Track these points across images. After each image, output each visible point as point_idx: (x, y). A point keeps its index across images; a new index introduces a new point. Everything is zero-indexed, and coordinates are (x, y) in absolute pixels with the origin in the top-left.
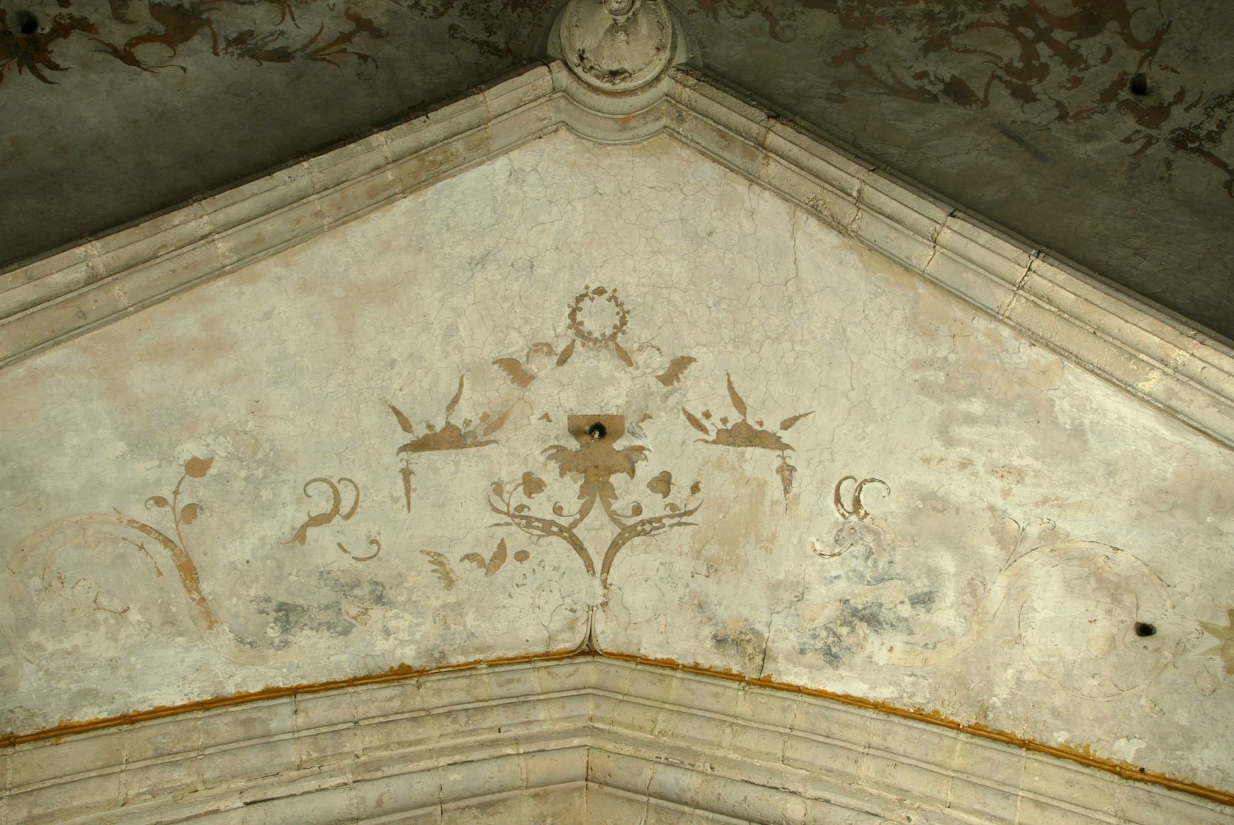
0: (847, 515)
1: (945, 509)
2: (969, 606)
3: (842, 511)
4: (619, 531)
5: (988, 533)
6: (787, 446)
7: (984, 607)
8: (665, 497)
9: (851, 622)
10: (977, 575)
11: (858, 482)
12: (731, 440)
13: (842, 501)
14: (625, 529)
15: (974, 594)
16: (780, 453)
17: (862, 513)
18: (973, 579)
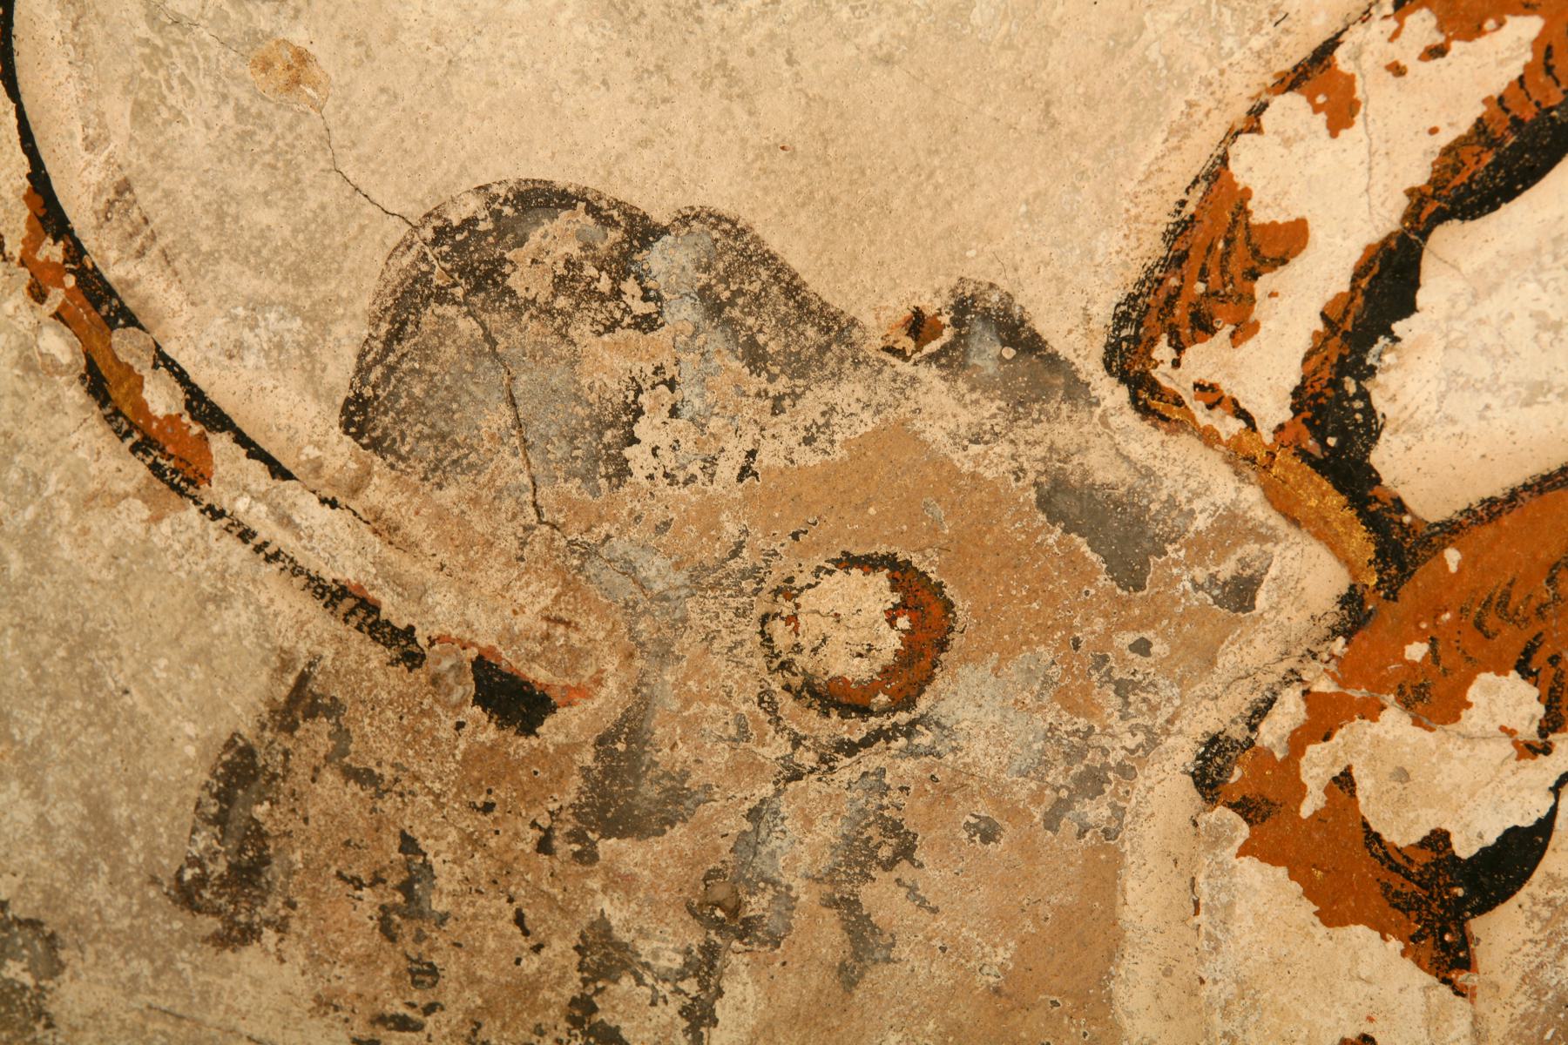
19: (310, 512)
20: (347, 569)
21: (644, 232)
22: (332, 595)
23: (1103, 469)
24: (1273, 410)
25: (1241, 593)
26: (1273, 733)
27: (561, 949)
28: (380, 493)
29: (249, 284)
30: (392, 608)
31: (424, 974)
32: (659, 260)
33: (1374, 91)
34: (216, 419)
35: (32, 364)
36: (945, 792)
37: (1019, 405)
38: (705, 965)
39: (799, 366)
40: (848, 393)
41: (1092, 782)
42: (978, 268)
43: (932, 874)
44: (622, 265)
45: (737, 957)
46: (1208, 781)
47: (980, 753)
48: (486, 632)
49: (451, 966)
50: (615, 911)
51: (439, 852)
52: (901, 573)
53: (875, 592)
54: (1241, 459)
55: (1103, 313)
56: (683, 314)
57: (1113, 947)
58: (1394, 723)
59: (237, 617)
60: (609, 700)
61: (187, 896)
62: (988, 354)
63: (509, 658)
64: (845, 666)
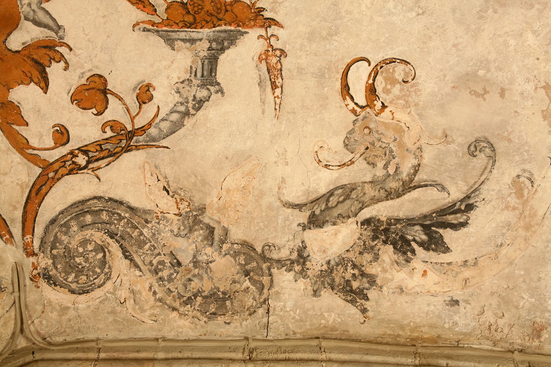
0: (359, 110)
1: (486, 92)
2: (514, 209)
3: (352, 105)
4: (38, 171)
5: (539, 118)
6: (272, 22)
7: (532, 208)
8: (99, 114)
9: (372, 248)
10: (524, 171)
11: (373, 64)
12: (189, 19)
13: (351, 92)
14: (47, 166)
15: (519, 193)
16: (262, 32)
17: (378, 105)
18: (518, 176)
19: (356, 156)
20: (359, 155)
21: (347, 137)
22: (360, 156)
23: (362, 118)
24: (361, 110)
25: (368, 113)
26: (375, 113)
27: (380, 149)
28: (356, 153)
29: (345, 157)
30: (362, 153)
31: (380, 156)
32: (348, 136)
33: (348, 103)
34: (351, 160)
35: (346, 169)
36: (375, 128)
37: (358, 121)
38: (382, 142)
39: (354, 131)
40: (356, 129)
41: (376, 121)
42: (352, 122)
43: (379, 130)
44: (348, 138)
45: (382, 140)
46: (377, 116)
47: (374, 126)
48: (364, 149)
49: (380, 155)
50: (378, 146)
51: (374, 154)
52: (365, 128)
53: (365, 130)
54: (362, 112)
55: (354, 116)
56: (351, 136)
57: (384, 122)
58: (376, 107)
59: (361, 161)
60: (368, 144)
61: (374, 167)
62: (355, 122)
63: (365, 148)
64: (368, 132)
